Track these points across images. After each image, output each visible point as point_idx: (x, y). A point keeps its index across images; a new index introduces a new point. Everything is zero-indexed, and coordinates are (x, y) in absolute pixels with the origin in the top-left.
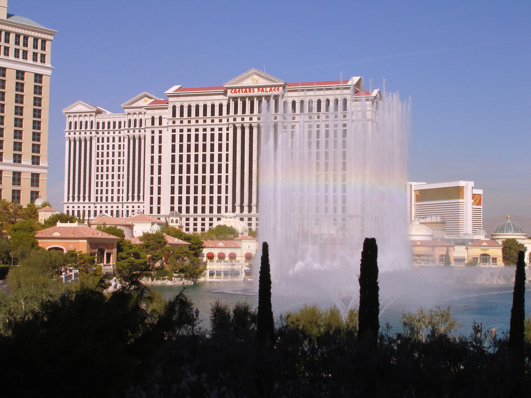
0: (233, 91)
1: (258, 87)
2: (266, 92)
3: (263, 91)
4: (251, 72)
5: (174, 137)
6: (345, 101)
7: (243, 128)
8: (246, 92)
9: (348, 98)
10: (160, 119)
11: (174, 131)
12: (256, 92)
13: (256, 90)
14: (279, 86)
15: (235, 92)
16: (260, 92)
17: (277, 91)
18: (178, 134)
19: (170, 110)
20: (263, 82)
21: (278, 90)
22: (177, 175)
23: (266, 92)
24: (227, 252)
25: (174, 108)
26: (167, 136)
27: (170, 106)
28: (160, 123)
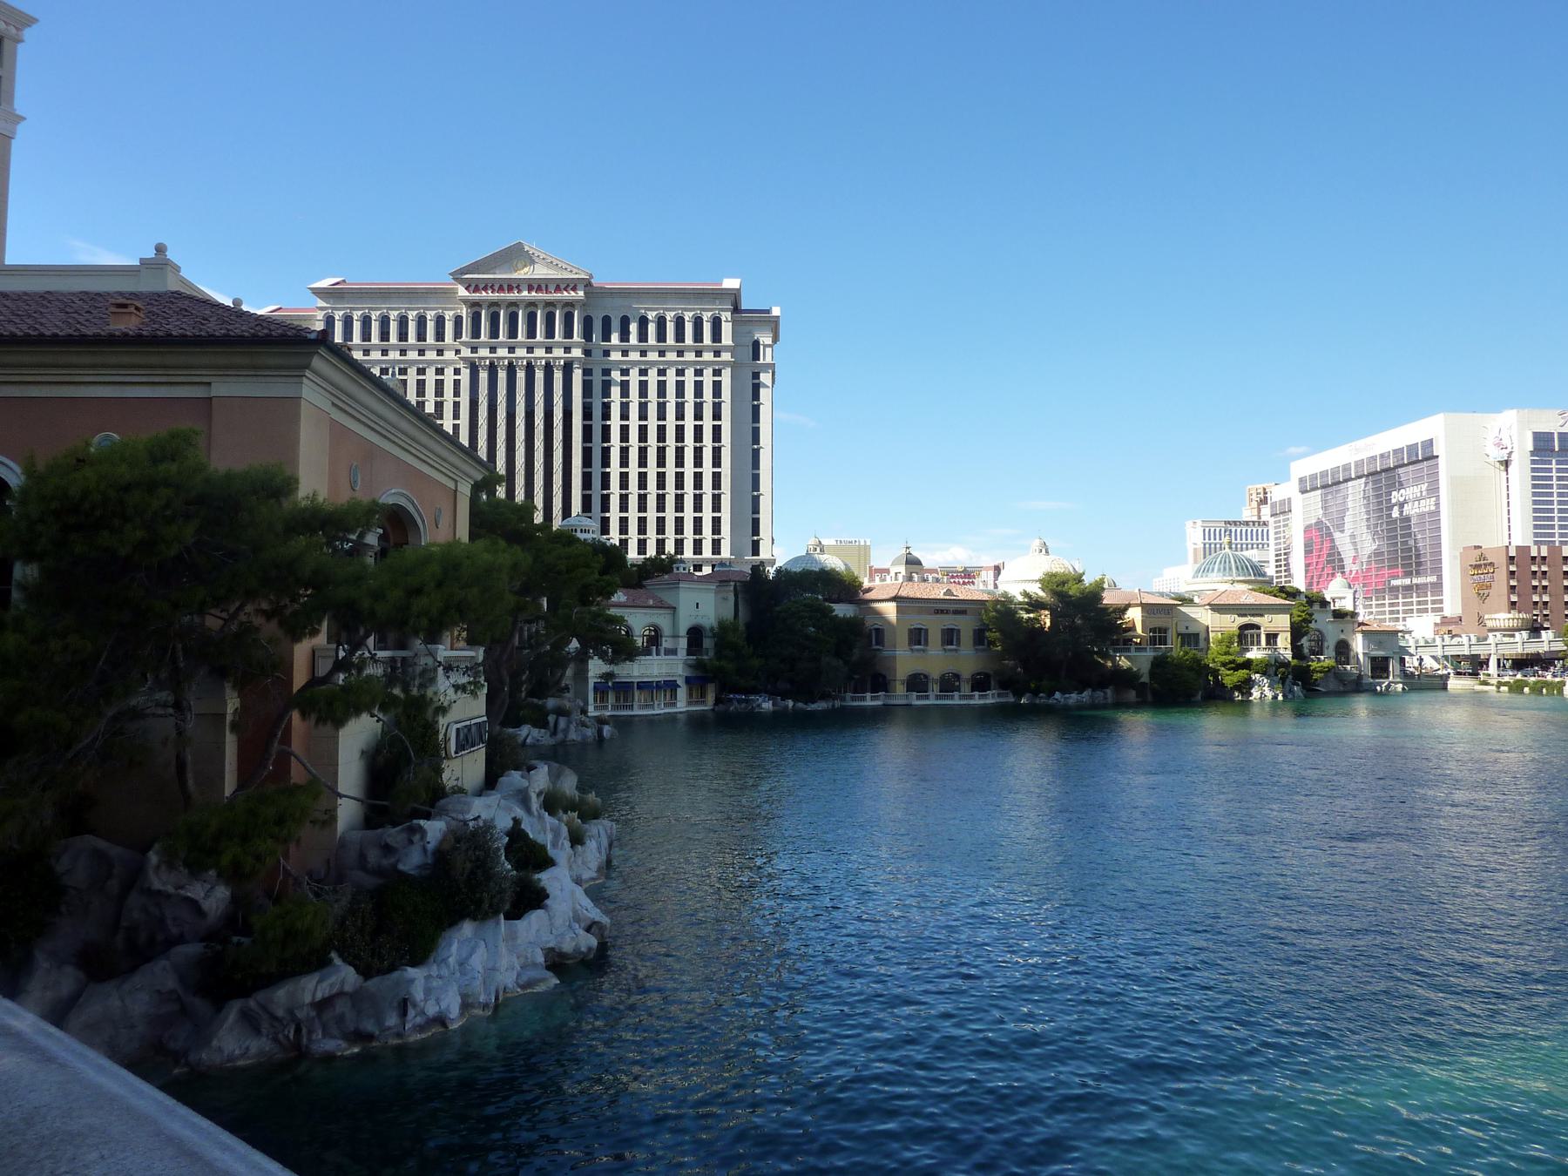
3: (539, 289)
6: (716, 324)
7: (493, 369)
15: (476, 290)
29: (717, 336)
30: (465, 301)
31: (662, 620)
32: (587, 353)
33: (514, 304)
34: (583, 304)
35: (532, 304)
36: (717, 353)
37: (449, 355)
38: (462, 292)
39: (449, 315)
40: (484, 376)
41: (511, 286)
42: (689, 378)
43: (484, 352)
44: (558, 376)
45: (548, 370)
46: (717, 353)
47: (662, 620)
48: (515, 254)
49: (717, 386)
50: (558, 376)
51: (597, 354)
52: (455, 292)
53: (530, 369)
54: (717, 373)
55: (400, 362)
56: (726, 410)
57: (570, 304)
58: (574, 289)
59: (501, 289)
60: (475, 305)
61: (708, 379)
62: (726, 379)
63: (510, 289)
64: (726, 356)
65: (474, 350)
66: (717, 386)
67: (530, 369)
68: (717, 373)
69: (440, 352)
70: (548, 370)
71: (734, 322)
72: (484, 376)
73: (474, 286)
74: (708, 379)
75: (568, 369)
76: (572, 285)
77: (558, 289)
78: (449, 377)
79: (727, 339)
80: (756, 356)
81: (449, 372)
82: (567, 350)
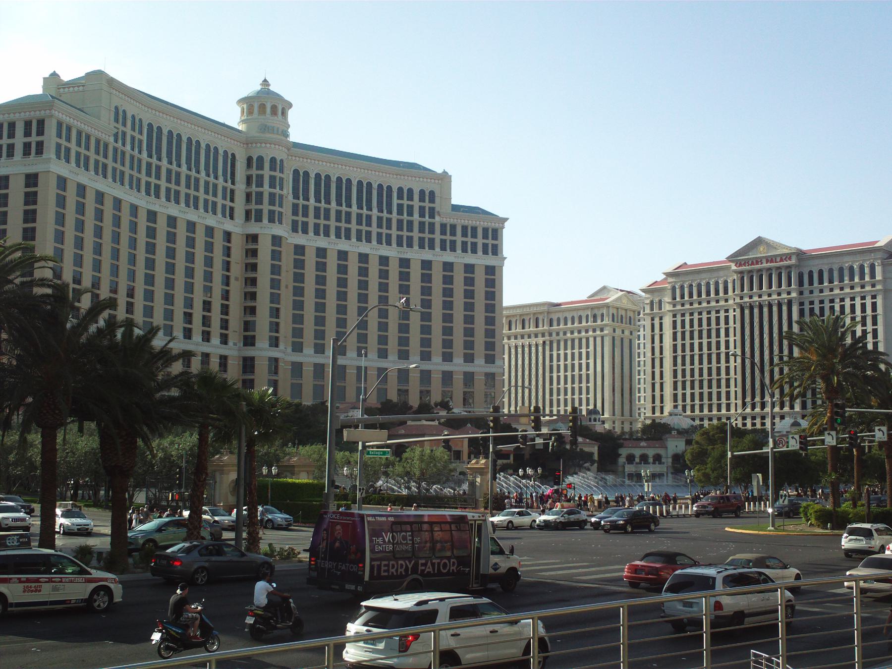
3: (772, 261)
5: (675, 322)
6: (872, 268)
7: (751, 308)
10: (660, 302)
11: (674, 316)
12: (765, 265)
13: (764, 261)
15: (740, 265)
18: (679, 319)
21: (790, 259)
22: (679, 368)
24: (651, 452)
25: (674, 289)
26: (667, 321)
28: (660, 309)
29: (873, 275)
30: (735, 272)
31: (661, 452)
32: (801, 293)
33: (760, 270)
34: (796, 266)
35: (769, 269)
36: (873, 286)
37: (731, 302)
38: (734, 267)
39: (730, 281)
40: (747, 312)
41: (758, 261)
42: (858, 302)
43: (746, 299)
44: (785, 308)
45: (780, 305)
46: (873, 286)
47: (661, 452)
48: (758, 242)
49: (874, 305)
50: (785, 308)
51: (806, 293)
52: (730, 267)
53: (770, 306)
54: (874, 297)
55: (707, 307)
56: (880, 320)
57: (789, 267)
58: (790, 259)
59: (752, 264)
60: (741, 272)
61: (869, 302)
62: (879, 301)
63: (757, 264)
64: (879, 287)
65: (742, 298)
66: (874, 305)
67: (770, 306)
68: (874, 297)
69: (726, 301)
70: (780, 305)
71: (883, 265)
72: (747, 312)
73: (739, 264)
74: (869, 302)
75: (790, 303)
76: (788, 256)
77: (781, 260)
78: (731, 314)
79: (879, 277)
81: (731, 311)
82: (789, 293)
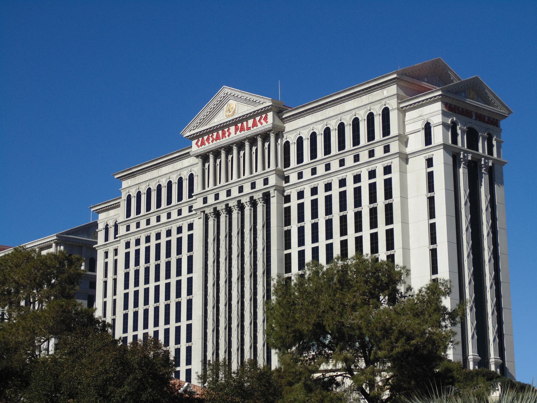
0: (199, 144)
1: (235, 123)
2: (249, 129)
3: (242, 129)
4: (222, 94)
6: (386, 113)
8: (218, 138)
9: (393, 104)
14: (265, 111)
16: (238, 133)
17: (264, 123)
19: (124, 204)
20: (244, 109)
23: (249, 129)
25: (129, 198)
27: (124, 196)
80: (428, 140)
